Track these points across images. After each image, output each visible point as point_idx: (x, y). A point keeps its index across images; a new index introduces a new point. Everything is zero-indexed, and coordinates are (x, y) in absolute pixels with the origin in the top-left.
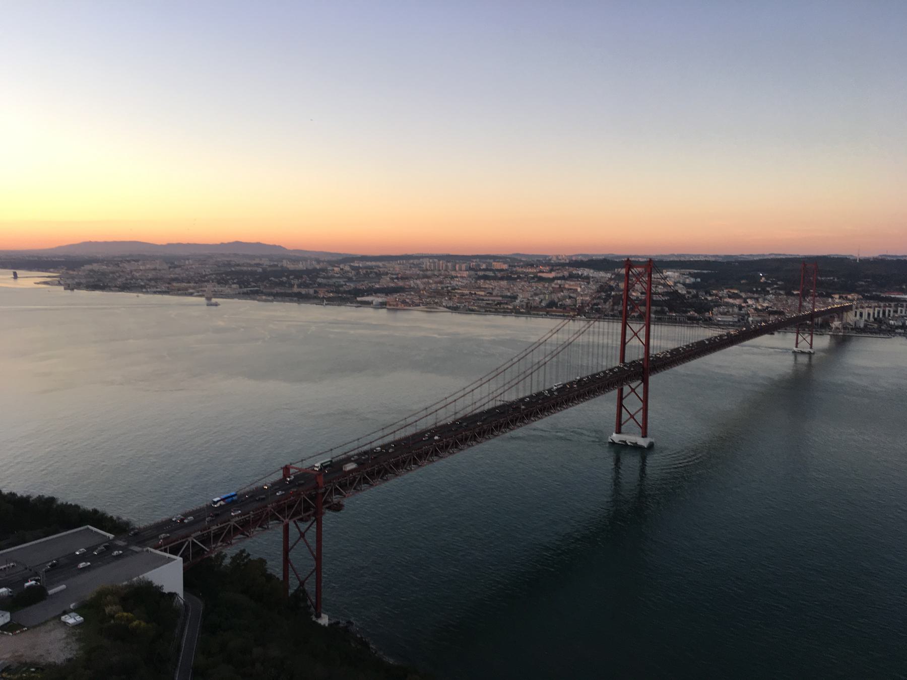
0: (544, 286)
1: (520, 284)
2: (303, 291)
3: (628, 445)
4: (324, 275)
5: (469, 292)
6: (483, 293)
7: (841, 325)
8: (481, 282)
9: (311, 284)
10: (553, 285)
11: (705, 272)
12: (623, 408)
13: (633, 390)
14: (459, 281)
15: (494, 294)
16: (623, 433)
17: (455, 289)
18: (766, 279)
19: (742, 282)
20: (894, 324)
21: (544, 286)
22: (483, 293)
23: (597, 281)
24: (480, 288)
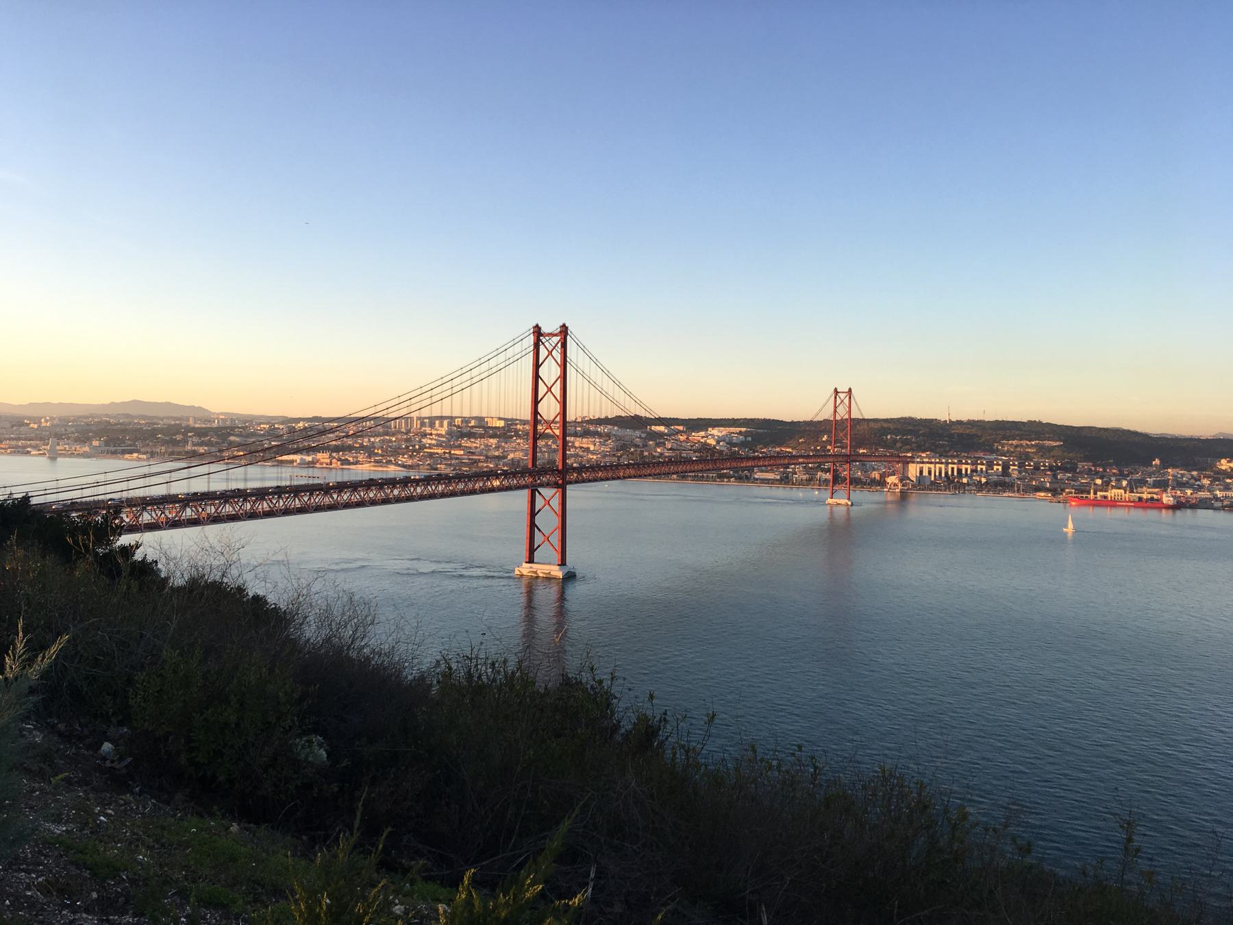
0: (546, 443)
2: (201, 450)
3: (537, 577)
4: (241, 432)
5: (443, 451)
6: (462, 452)
8: (465, 442)
9: (217, 443)
11: (759, 431)
14: (432, 439)
17: (423, 447)
19: (800, 441)
20: (968, 481)
22: (462, 452)
23: (618, 438)
24: (459, 447)
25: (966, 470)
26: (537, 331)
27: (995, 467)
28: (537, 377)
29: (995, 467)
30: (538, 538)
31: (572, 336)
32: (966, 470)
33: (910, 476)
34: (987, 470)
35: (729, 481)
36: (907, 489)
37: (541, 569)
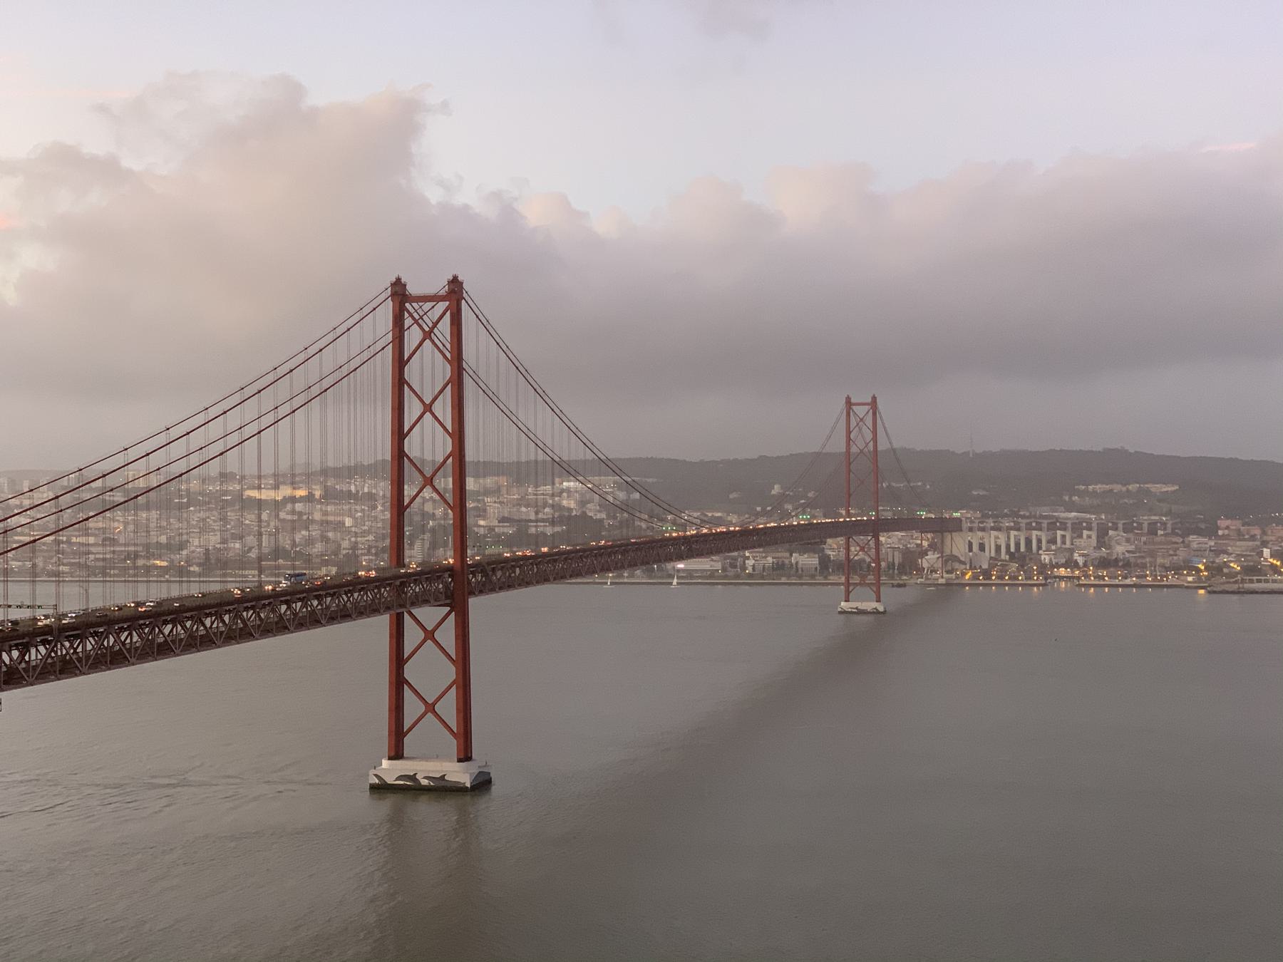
1: (195, 515)
7: (940, 559)
10: (282, 515)
11: (650, 480)
12: (405, 686)
13: (430, 635)
15: (122, 540)
16: (408, 758)
18: (782, 488)
20: (1051, 560)
21: (259, 516)
22: (92, 540)
25: (1039, 541)
26: (399, 293)
27: (1085, 533)
28: (400, 383)
29: (1085, 533)
30: (412, 708)
31: (470, 302)
32: (1039, 541)
33: (955, 552)
34: (1072, 539)
35: (631, 576)
36: (957, 578)
37: (424, 769)
